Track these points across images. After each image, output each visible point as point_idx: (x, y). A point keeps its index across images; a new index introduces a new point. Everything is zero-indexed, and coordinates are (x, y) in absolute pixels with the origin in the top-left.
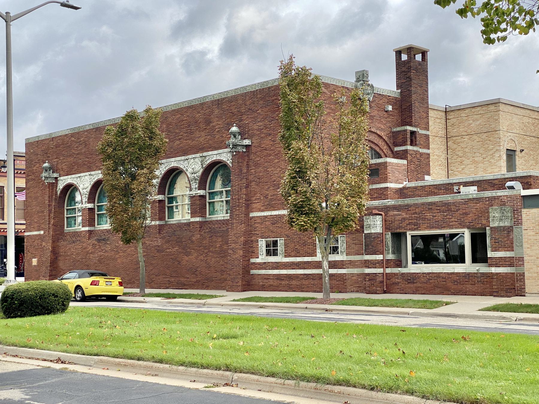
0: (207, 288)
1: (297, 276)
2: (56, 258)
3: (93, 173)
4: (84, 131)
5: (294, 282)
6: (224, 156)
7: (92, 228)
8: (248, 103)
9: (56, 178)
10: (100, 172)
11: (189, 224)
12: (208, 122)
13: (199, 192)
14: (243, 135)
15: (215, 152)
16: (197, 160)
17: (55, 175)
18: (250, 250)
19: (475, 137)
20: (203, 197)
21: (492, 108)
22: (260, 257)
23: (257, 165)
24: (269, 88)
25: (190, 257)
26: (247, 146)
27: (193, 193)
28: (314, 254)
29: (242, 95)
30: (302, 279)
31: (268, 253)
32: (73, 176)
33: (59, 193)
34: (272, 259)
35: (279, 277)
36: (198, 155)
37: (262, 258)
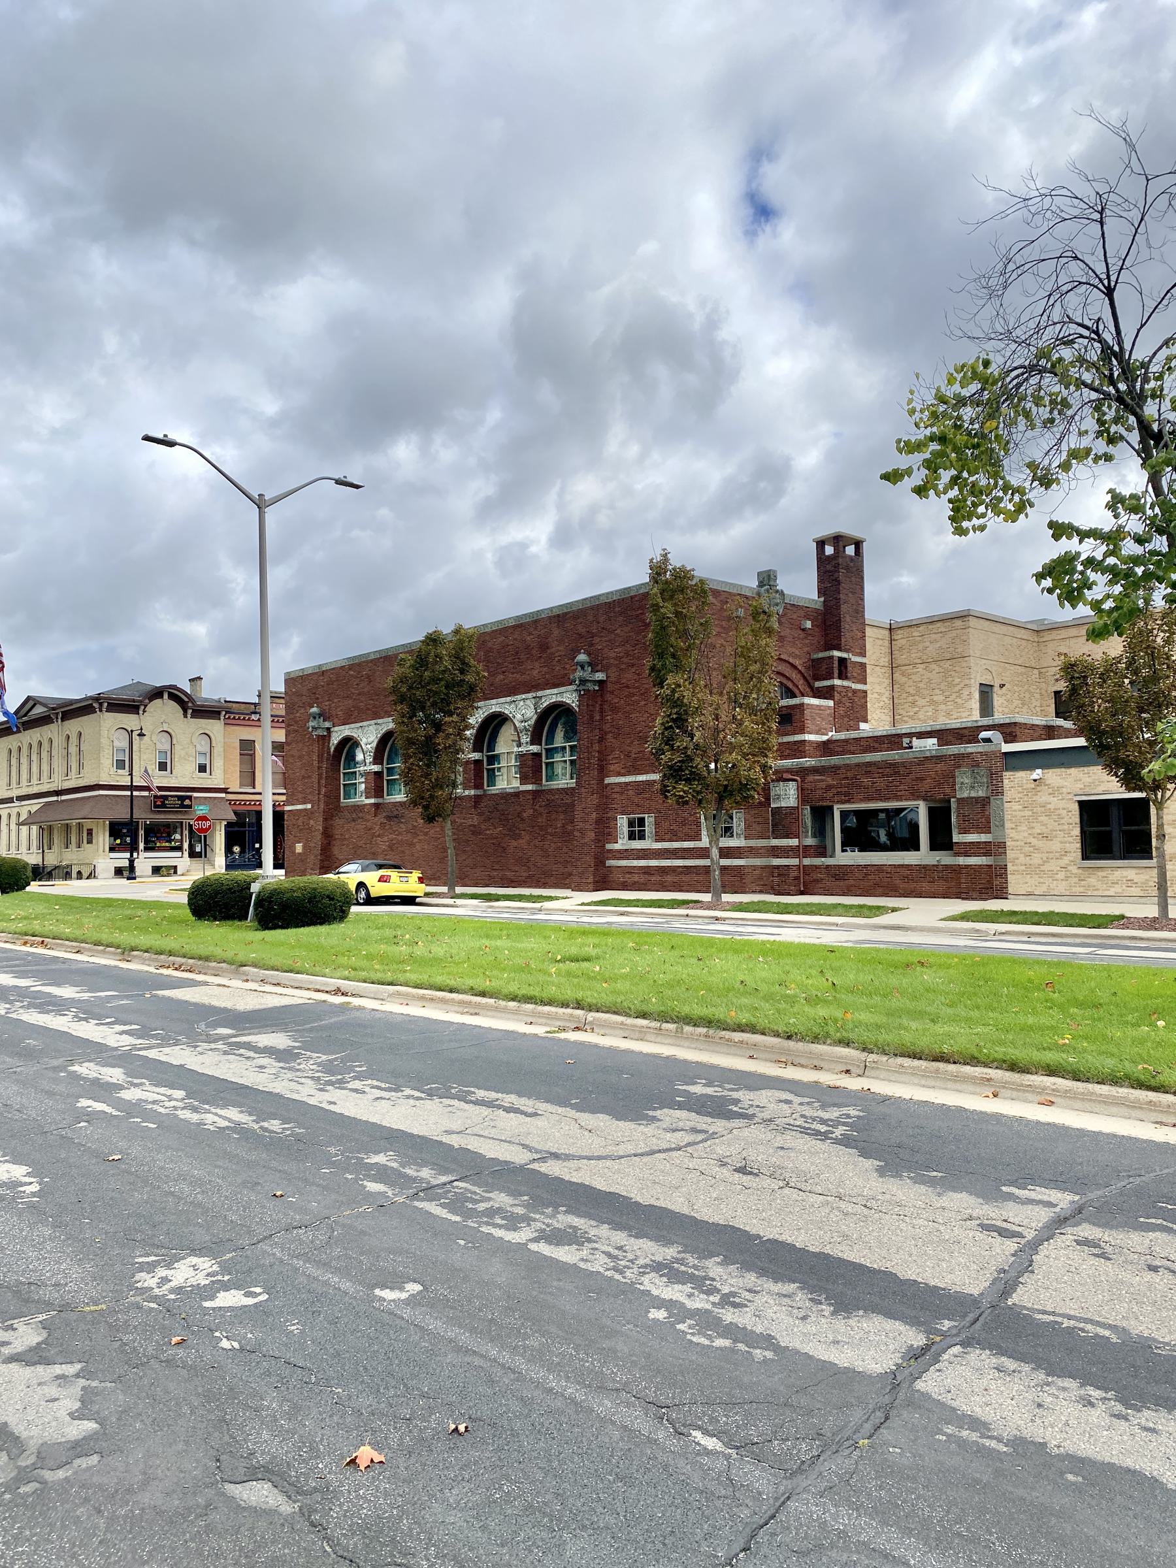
0: (545, 885)
1: (673, 869)
2: (329, 844)
3: (380, 721)
4: (367, 662)
5: (669, 878)
6: (568, 696)
7: (380, 800)
8: (602, 619)
9: (328, 729)
10: (390, 719)
11: (517, 794)
12: (544, 647)
13: (531, 747)
14: (594, 666)
15: (555, 691)
16: (528, 702)
17: (327, 724)
18: (606, 831)
19: (933, 666)
20: (537, 755)
21: (958, 623)
22: (620, 841)
23: (615, 709)
24: (632, 597)
25: (520, 841)
26: (601, 683)
27: (523, 749)
28: (697, 837)
29: (592, 608)
30: (681, 873)
31: (632, 836)
32: (352, 726)
33: (332, 749)
34: (637, 844)
35: (647, 871)
36: (530, 695)
37: (622, 843)
